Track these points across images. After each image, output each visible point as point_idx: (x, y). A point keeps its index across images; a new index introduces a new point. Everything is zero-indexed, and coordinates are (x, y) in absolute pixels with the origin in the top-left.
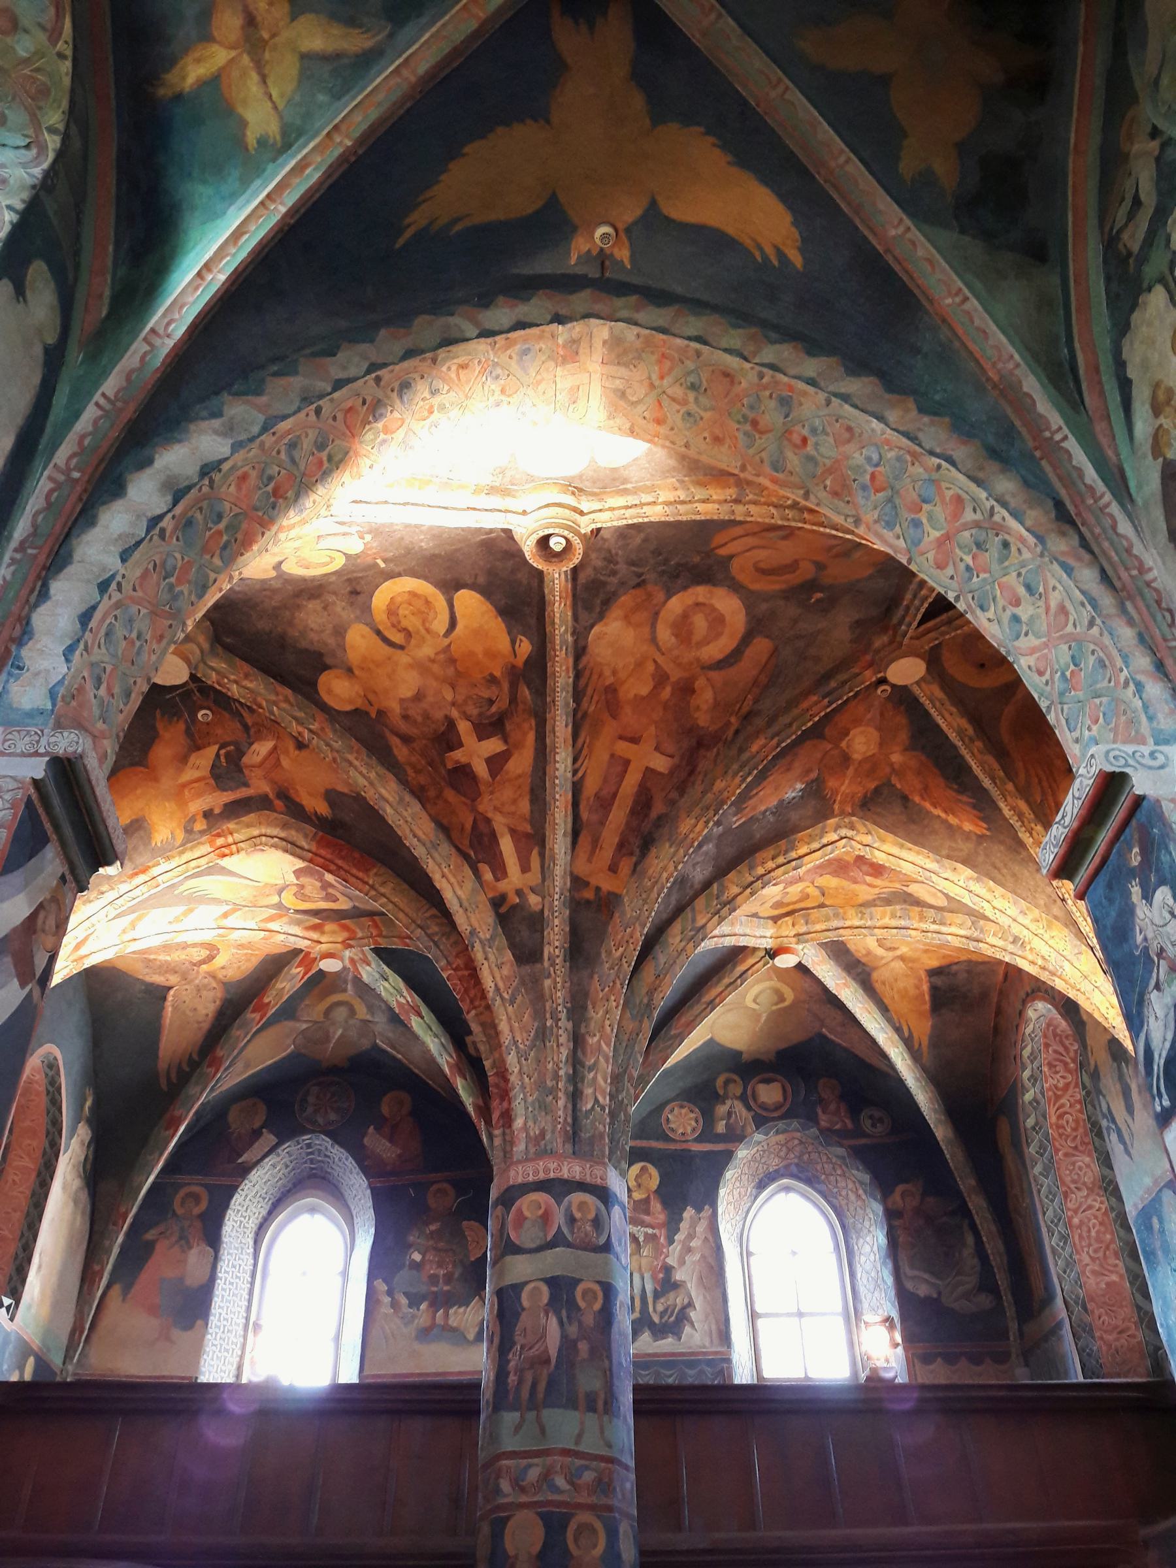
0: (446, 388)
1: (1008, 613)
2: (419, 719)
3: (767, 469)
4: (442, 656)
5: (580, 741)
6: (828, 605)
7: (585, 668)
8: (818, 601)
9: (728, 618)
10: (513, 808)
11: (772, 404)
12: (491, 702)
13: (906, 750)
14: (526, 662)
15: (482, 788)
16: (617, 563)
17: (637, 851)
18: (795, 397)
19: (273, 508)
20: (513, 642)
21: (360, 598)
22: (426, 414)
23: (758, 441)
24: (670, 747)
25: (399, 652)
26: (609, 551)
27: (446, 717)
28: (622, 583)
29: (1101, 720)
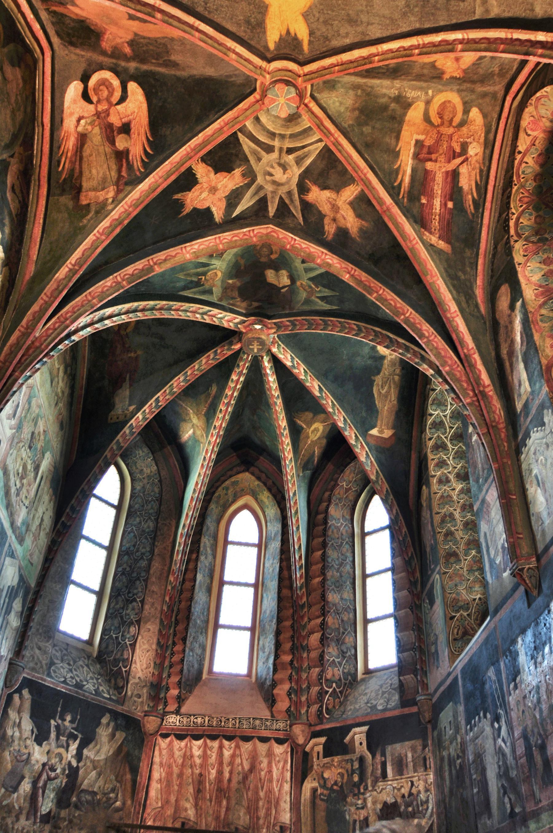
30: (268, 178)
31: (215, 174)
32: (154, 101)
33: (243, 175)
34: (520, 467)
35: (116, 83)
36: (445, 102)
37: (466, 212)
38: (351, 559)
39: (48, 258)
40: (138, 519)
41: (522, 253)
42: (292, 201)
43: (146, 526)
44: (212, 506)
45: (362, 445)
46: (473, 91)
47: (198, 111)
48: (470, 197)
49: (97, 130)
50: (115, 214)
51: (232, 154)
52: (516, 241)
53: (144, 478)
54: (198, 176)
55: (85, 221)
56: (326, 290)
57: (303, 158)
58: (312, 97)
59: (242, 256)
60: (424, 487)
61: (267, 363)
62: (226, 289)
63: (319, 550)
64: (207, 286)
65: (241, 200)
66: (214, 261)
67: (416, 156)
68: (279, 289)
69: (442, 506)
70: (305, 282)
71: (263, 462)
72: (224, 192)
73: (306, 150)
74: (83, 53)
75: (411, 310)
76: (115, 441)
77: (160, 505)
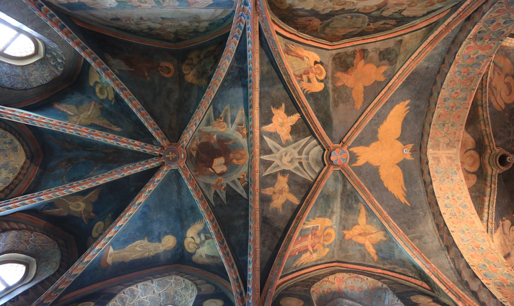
0: (447, 194)
3: (467, 101)
11: (446, 103)
18: (443, 98)
19: (483, 249)
22: (454, 201)
30: (284, 153)
31: (291, 126)
32: (320, 95)
33: (287, 141)
35: (322, 77)
36: (331, 235)
42: (274, 168)
46: (335, 246)
49: (306, 66)
51: (300, 134)
53: (25, 76)
54: (292, 117)
56: (225, 196)
57: (299, 171)
59: (234, 143)
62: (209, 134)
64: (214, 122)
65: (273, 140)
66: (234, 126)
67: (313, 228)
72: (279, 131)
73: (304, 172)
74: (330, 63)
77: (9, 88)
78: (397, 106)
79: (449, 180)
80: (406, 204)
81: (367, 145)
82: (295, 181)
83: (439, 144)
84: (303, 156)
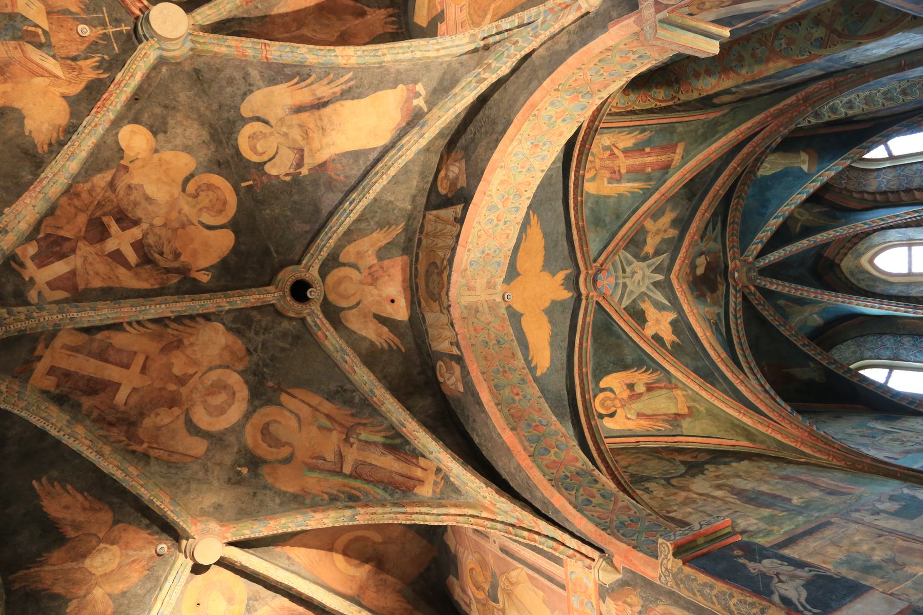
0: (503, 228)
1: (584, 497)
2: (132, 198)
3: (492, 384)
4: (185, 219)
5: (149, 325)
6: (235, 480)
7: (197, 322)
8: (239, 473)
9: (223, 417)
10: (91, 273)
12: (161, 254)
13: (109, 595)
14: (194, 279)
15: (98, 246)
16: (264, 334)
17: (58, 391)
20: (206, 269)
21: (216, 167)
23: (499, 376)
24: (132, 402)
25: (180, 189)
26: (273, 328)
27: (140, 219)
28: (250, 340)
29: (653, 538)
30: (641, 284)
32: (610, 369)
33: (644, 301)
34: (873, 63)
35: (601, 396)
37: (650, 137)
38: (919, 165)
39: (732, 432)
40: (901, 351)
41: (690, 94)
43: (908, 344)
44: (878, 290)
45: (820, 176)
47: (613, 338)
48: (638, 136)
49: (634, 406)
50: (696, 388)
52: (679, 99)
55: (702, 409)
58: (595, 261)
60: (855, 119)
61: (763, 262)
63: (914, 195)
64: (716, 318)
67: (618, 181)
68: (708, 263)
69: (876, 103)
70: (704, 244)
71: (827, 253)
73: (623, 260)
75: (732, 164)
76: (845, 376)
78: (548, 365)
79: (487, 251)
80: (534, 213)
81: (554, 303)
82: (637, 246)
83: (490, 311)
84: (621, 281)
